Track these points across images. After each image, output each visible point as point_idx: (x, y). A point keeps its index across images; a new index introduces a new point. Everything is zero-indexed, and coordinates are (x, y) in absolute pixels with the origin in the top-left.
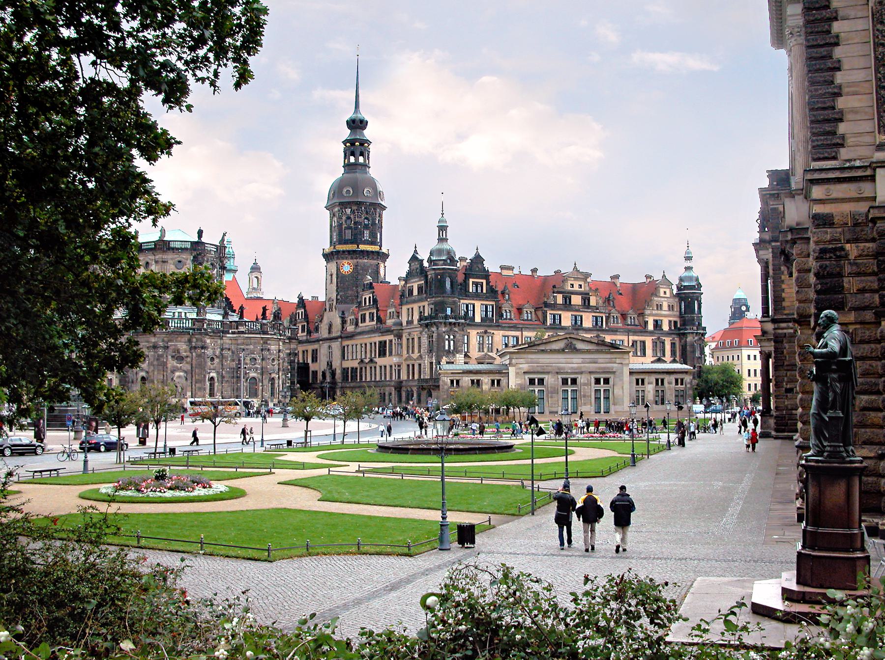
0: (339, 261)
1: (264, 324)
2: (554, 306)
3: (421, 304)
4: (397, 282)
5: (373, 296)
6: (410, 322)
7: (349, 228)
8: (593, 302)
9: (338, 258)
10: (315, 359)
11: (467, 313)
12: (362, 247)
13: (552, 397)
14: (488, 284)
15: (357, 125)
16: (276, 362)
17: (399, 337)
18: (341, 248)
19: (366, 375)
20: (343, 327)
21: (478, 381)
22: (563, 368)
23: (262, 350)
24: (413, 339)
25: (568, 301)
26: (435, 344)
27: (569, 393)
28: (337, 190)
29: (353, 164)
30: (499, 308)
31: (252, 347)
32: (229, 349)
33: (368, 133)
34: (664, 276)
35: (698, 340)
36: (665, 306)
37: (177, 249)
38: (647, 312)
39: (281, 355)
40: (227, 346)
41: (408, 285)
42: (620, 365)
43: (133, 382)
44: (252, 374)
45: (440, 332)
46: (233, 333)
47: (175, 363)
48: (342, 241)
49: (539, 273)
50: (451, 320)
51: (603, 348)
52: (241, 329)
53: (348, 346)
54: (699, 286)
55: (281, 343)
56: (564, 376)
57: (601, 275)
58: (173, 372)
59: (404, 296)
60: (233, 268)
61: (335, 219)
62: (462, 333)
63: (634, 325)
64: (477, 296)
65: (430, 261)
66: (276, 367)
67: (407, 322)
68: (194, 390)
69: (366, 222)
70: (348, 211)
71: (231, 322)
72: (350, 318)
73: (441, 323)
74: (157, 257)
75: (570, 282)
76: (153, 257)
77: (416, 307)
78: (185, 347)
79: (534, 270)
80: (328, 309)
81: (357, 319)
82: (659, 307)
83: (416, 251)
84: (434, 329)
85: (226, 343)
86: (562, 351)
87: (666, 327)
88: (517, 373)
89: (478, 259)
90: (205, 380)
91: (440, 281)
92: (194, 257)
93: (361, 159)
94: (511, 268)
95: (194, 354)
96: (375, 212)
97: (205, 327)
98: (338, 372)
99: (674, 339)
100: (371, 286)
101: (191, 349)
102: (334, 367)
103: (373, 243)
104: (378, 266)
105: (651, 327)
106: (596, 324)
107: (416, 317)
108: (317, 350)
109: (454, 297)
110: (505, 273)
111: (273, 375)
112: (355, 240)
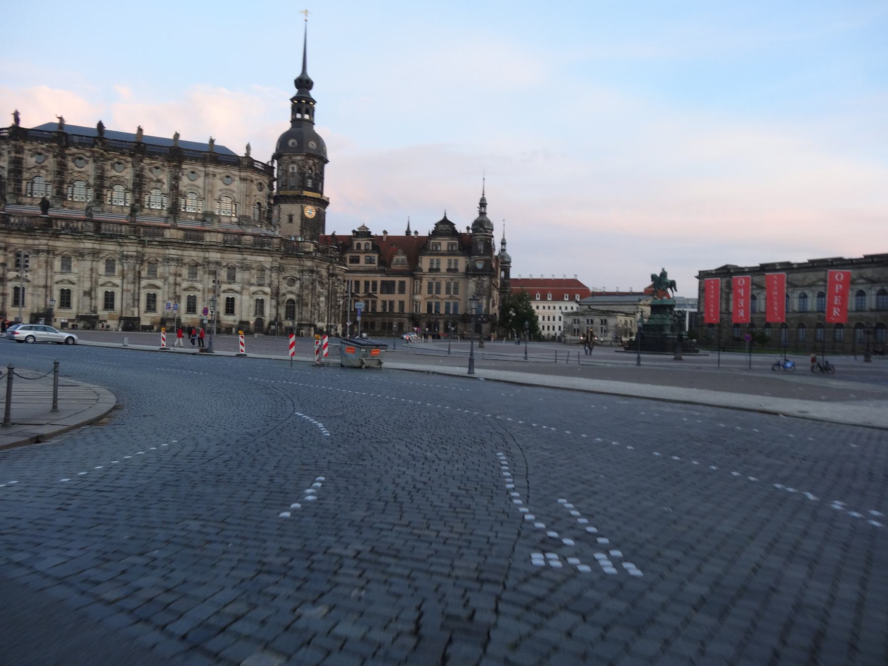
0: (304, 205)
3: (453, 258)
4: (381, 234)
5: (373, 245)
7: (310, 177)
15: (304, 84)
18: (306, 193)
33: (313, 93)
58: (319, 297)
61: (295, 166)
67: (431, 270)
74: (243, 174)
83: (445, 217)
95: (331, 281)
101: (329, 276)
107: (444, 266)
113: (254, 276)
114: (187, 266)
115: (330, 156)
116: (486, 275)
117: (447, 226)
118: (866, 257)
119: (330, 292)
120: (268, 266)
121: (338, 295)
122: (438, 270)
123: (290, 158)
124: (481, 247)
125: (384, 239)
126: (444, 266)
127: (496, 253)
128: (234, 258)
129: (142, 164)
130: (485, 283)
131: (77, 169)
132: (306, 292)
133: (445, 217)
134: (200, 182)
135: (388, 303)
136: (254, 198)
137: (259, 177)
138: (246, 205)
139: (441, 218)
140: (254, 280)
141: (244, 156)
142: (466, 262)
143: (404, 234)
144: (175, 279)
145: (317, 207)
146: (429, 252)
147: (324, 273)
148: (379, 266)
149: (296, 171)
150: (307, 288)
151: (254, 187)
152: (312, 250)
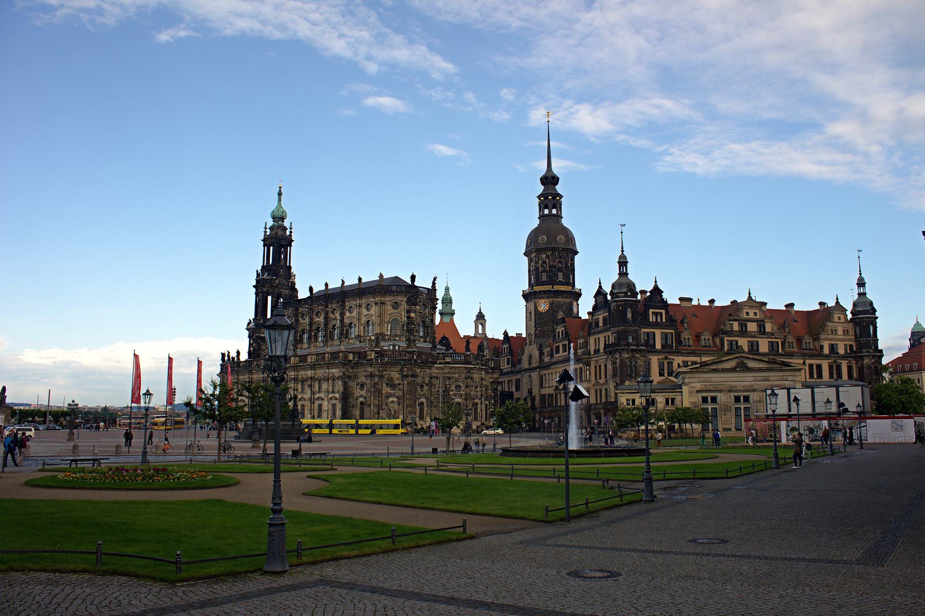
0: (536, 301)
1: (468, 356)
2: (731, 333)
3: (606, 334)
5: (565, 329)
6: (597, 351)
7: (544, 271)
8: (768, 328)
9: (536, 298)
10: (518, 389)
11: (647, 342)
12: (556, 288)
13: (725, 414)
14: (666, 314)
15: (550, 180)
16: (479, 389)
17: (588, 364)
18: (537, 289)
19: (560, 400)
20: (541, 359)
21: (653, 400)
22: (736, 387)
23: (466, 378)
24: (600, 366)
25: (744, 328)
26: (619, 370)
27: (742, 411)
28: (533, 238)
30: (678, 336)
31: (457, 375)
32: (437, 378)
34: (837, 303)
35: (875, 362)
36: (840, 332)
37: (394, 292)
38: (823, 336)
39: (484, 383)
40: (435, 375)
41: (594, 318)
42: (792, 382)
43: (353, 407)
44: (458, 400)
45: (623, 358)
46: (440, 363)
47: (389, 390)
48: (539, 282)
49: (716, 304)
50: (632, 347)
51: (775, 366)
52: (448, 360)
53: (545, 375)
54: (874, 311)
55: (483, 373)
56: (736, 394)
57: (776, 304)
58: (387, 397)
59: (589, 326)
60: (450, 311)
61: (533, 264)
62: (644, 358)
63: (810, 349)
64: (656, 325)
65: (612, 293)
66: (479, 394)
68: (405, 414)
69: (560, 265)
70: (544, 256)
71: (439, 354)
72: (546, 350)
73: (623, 350)
74: (377, 299)
75: (745, 311)
77: (601, 336)
78: (397, 376)
79: (712, 301)
80: (528, 343)
81: (552, 350)
82: (834, 332)
83: (600, 287)
84: (617, 356)
85: (434, 373)
86: (733, 370)
87: (841, 351)
88: (690, 392)
89: (657, 291)
90: (415, 405)
91: (621, 311)
92: (407, 299)
93: (554, 211)
94: (690, 300)
95: (405, 382)
96: (568, 256)
97: (415, 358)
98: (537, 398)
99: (850, 362)
100: (563, 320)
102: (533, 394)
103: (567, 284)
104: (571, 304)
105: (826, 351)
106: (773, 349)
108: (519, 379)
109: (635, 327)
110: (685, 304)
111: (476, 401)
112: (552, 281)
114: (300, 383)
117: (601, 297)
119: (405, 392)
121: (451, 393)
122: (599, 350)
128: (320, 373)
129: (327, 309)
131: (303, 322)
133: (600, 287)
134: (354, 314)
140: (330, 389)
144: (294, 393)
147: (396, 375)
152: (373, 357)
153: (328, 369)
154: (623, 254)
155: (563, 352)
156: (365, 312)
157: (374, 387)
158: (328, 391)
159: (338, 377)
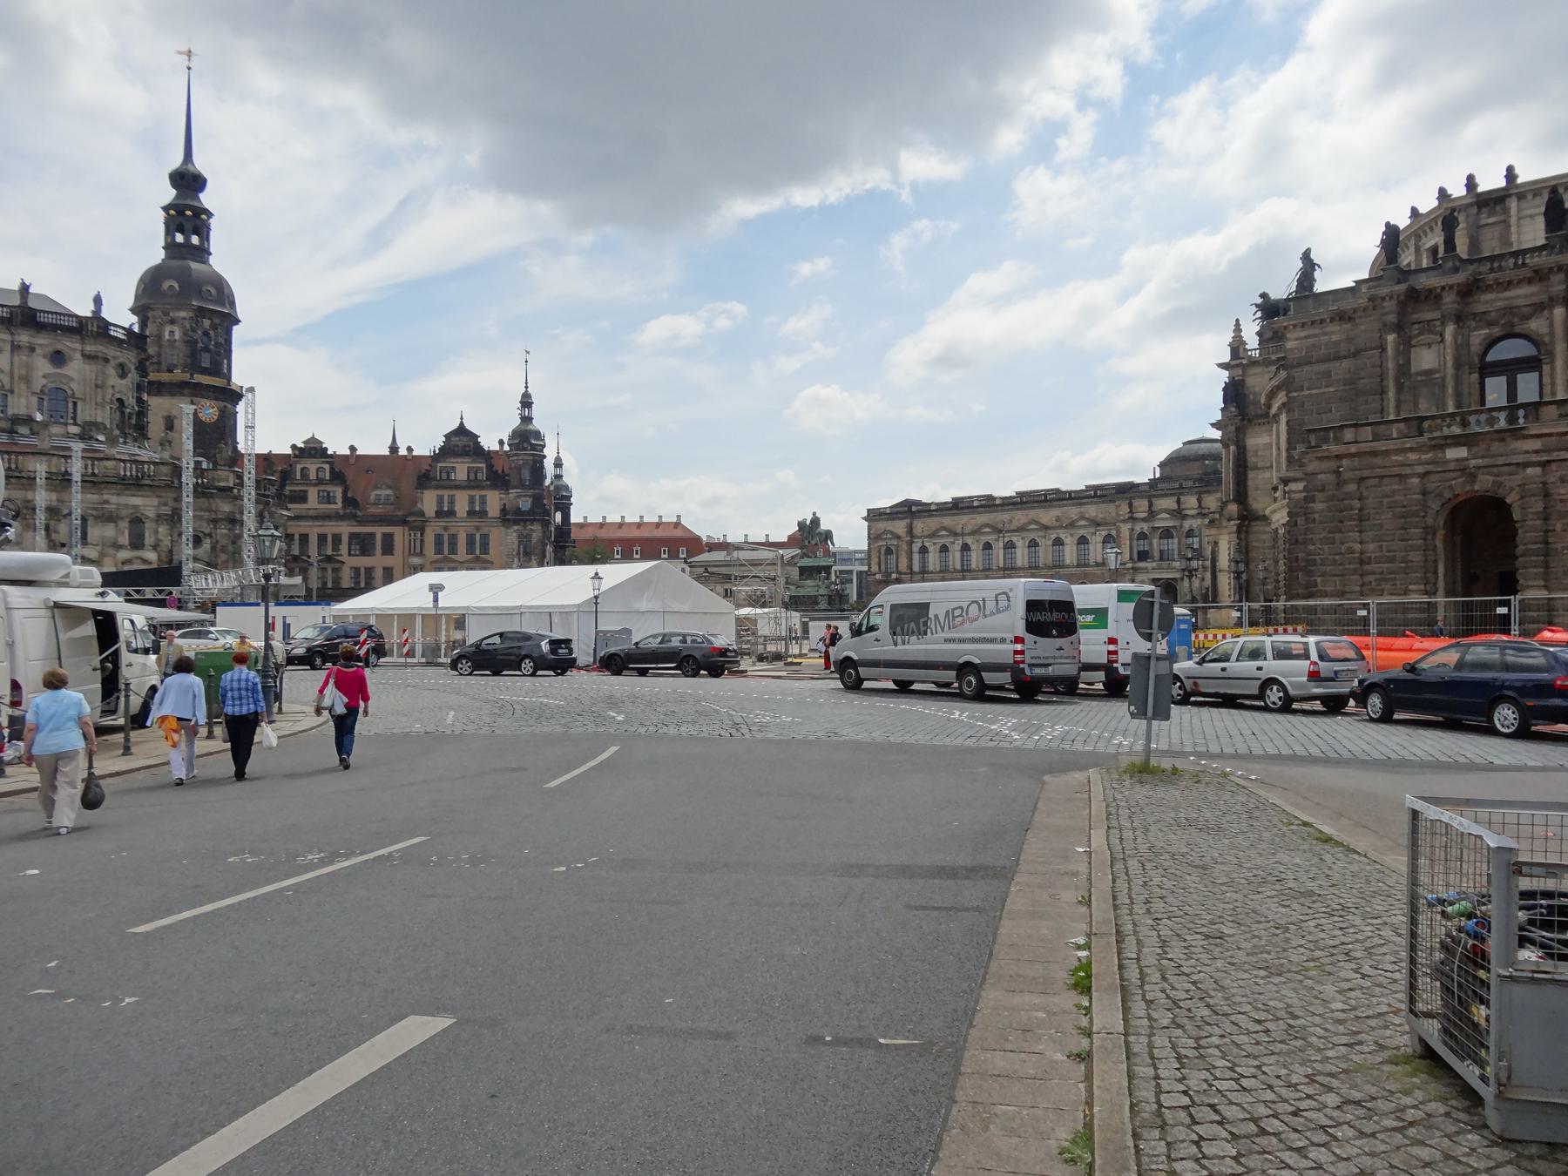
3: (477, 493)
5: (332, 470)
6: (445, 514)
7: (206, 349)
9: (193, 395)
15: (188, 181)
29: (195, 247)
33: (207, 199)
67: (440, 514)
74: (91, 348)
76: (78, 346)
83: (462, 423)
107: (462, 507)
113: (123, 533)
115: (241, 311)
116: (535, 520)
117: (465, 439)
118: (1089, 488)
120: (151, 514)
123: (166, 314)
124: (526, 475)
125: (352, 461)
126: (462, 507)
127: (547, 482)
130: (534, 534)
132: (223, 557)
133: (462, 423)
135: (362, 571)
136: (110, 391)
137: (119, 354)
138: (96, 404)
139: (455, 425)
140: (124, 539)
141: (90, 315)
142: (501, 499)
143: (386, 452)
145: (222, 404)
146: (434, 483)
148: (344, 507)
149: (177, 337)
150: (224, 549)
151: (111, 371)
152: (231, 485)
153: (118, 494)
154: (527, 391)
155: (319, 503)
156: (43, 366)
157: (234, 543)
158: (115, 543)
159: (159, 516)
